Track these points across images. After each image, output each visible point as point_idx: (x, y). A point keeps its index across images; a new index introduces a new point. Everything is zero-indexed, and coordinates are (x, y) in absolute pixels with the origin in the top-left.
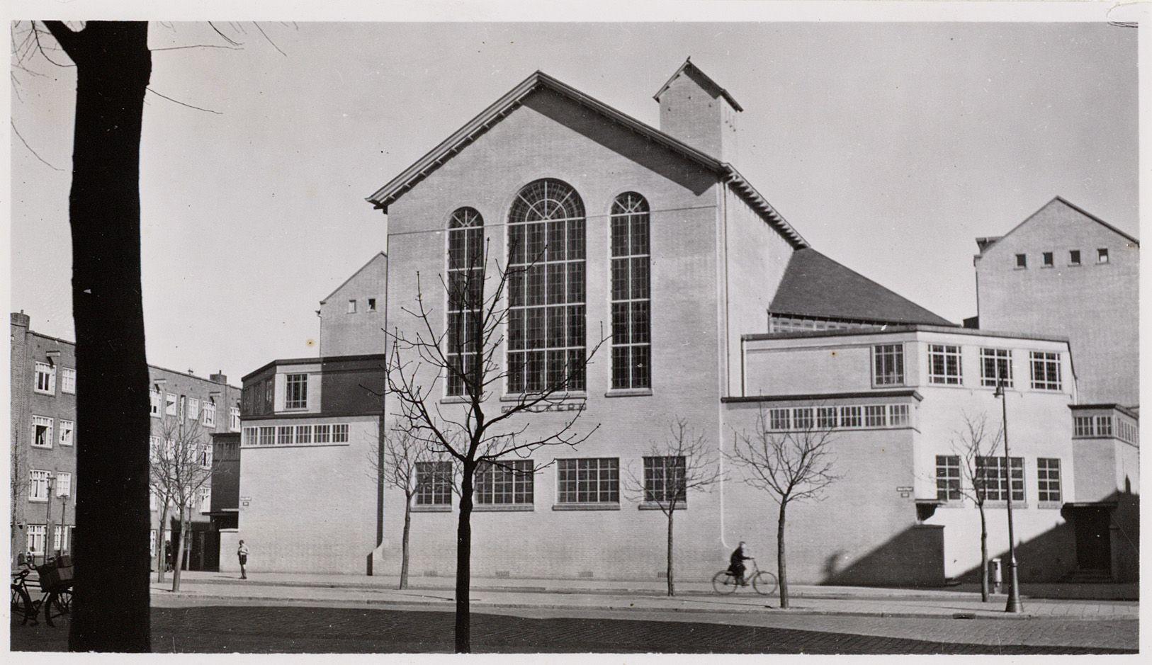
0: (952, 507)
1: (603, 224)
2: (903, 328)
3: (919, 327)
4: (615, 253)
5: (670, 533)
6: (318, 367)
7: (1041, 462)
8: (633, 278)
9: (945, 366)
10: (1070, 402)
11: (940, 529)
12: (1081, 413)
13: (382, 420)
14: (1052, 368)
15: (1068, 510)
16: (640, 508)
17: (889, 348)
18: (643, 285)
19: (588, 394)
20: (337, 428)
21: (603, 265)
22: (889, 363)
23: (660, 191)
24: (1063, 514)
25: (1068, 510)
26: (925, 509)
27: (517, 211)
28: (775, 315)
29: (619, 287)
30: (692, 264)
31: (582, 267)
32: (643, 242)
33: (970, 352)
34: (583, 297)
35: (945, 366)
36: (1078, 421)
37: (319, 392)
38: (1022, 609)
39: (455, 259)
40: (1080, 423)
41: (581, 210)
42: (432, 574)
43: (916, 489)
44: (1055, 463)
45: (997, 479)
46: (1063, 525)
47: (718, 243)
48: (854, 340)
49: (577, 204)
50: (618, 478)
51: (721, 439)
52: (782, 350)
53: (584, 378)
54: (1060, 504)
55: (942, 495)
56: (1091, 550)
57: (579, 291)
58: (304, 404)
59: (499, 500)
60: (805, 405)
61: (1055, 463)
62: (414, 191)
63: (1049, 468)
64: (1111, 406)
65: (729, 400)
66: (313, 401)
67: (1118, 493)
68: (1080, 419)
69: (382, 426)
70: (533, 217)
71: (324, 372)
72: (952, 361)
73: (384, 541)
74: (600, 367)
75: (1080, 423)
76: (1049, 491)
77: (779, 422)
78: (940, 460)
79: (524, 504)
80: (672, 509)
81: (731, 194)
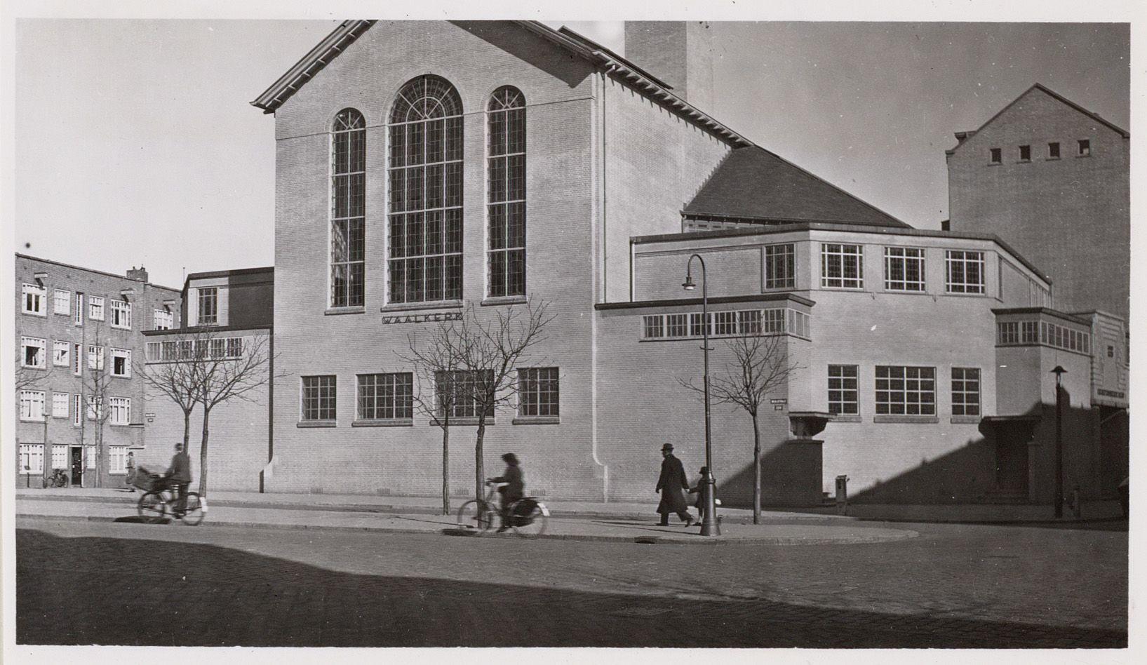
0: (846, 421)
1: (480, 121)
2: (795, 226)
3: (811, 225)
4: (493, 152)
5: (445, 447)
6: (225, 281)
7: (957, 373)
8: (509, 177)
9: (843, 268)
10: (994, 307)
11: (820, 443)
12: (1006, 319)
13: (272, 333)
14: (973, 269)
15: (986, 424)
16: (515, 423)
17: (780, 248)
18: (519, 187)
19: (464, 303)
20: (231, 342)
21: (480, 165)
22: (781, 266)
23: (539, 88)
24: (980, 430)
25: (986, 424)
26: (813, 423)
27: (399, 111)
28: (689, 217)
29: (496, 190)
30: (566, 162)
31: (460, 166)
32: (519, 139)
33: (874, 252)
34: (460, 201)
35: (843, 268)
36: (1002, 327)
37: (227, 306)
38: (718, 532)
39: (340, 165)
40: (1005, 330)
41: (460, 109)
42: (318, 492)
43: (789, 402)
44: (974, 373)
45: (904, 393)
46: (980, 442)
47: (594, 138)
48: (745, 240)
49: (455, 101)
50: (557, 389)
51: (595, 349)
52: (671, 252)
53: (461, 286)
54: (978, 418)
55: (834, 409)
56: (1048, 471)
57: (457, 192)
58: (215, 318)
59: (381, 415)
60: (677, 311)
61: (974, 373)
62: (299, 93)
63: (966, 381)
64: (1038, 310)
65: (603, 307)
66: (222, 318)
67: (1041, 406)
68: (1005, 325)
69: (173, 332)
70: (414, 116)
71: (231, 286)
72: (851, 263)
73: (274, 457)
74: (477, 274)
75: (1005, 330)
76: (965, 402)
77: (653, 330)
78: (833, 370)
79: (405, 419)
80: (446, 424)
81: (615, 88)
